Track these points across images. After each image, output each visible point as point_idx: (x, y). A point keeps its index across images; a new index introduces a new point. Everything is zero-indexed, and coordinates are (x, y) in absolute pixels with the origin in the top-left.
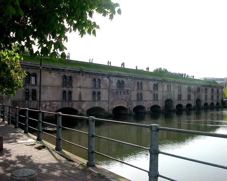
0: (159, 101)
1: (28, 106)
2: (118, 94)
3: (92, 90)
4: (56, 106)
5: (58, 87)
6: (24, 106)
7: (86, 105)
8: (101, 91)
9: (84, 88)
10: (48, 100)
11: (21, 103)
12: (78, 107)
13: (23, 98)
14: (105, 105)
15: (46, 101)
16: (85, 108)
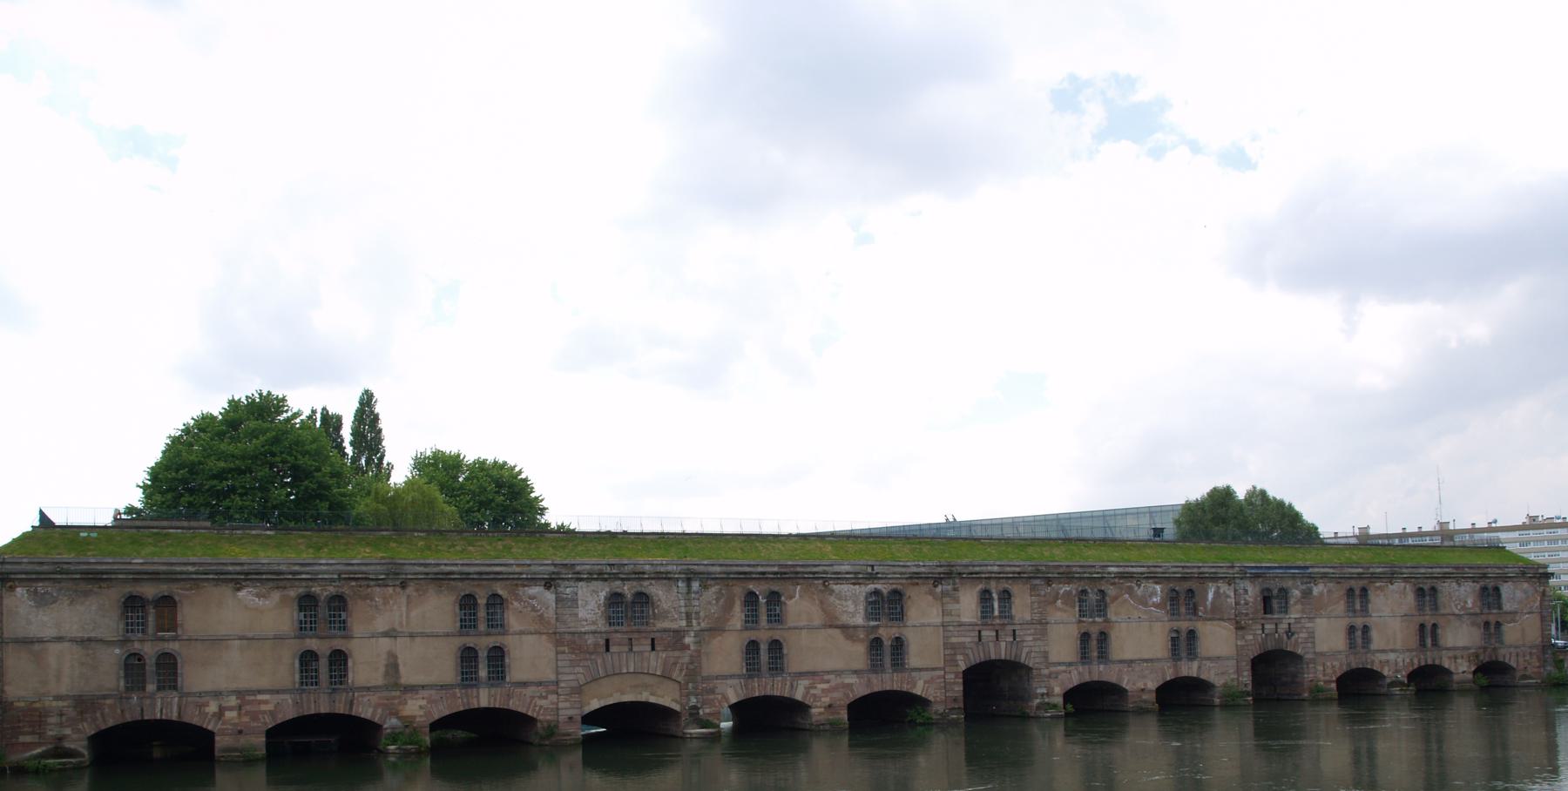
0: (914, 674)
1: (142, 710)
2: (613, 649)
3: (459, 642)
4: (270, 707)
5: (278, 638)
6: (122, 711)
7: (424, 703)
8: (509, 642)
9: (412, 636)
10: (234, 686)
11: (109, 702)
12: (379, 711)
13: (119, 686)
14: (533, 698)
15: (221, 693)
16: (422, 713)
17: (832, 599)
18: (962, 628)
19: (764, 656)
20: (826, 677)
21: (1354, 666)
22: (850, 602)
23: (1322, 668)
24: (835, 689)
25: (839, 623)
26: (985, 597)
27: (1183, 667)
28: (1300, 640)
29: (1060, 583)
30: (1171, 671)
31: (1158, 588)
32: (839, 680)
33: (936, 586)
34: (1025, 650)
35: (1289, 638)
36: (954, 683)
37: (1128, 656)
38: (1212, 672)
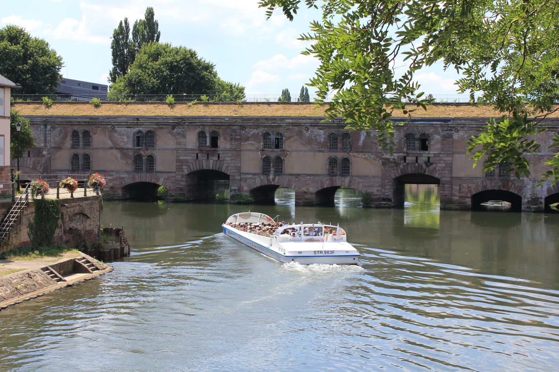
0: (158, 174)
17: (116, 135)
18: (186, 152)
19: (81, 162)
20: (111, 173)
21: (489, 187)
22: (125, 137)
23: (458, 188)
24: (115, 179)
25: (119, 147)
26: (202, 135)
27: (337, 181)
28: (437, 168)
29: (251, 128)
30: (327, 182)
31: (322, 132)
32: (118, 175)
33: (173, 129)
34: (225, 165)
35: (427, 166)
36: (181, 180)
37: (296, 172)
38: (361, 185)
